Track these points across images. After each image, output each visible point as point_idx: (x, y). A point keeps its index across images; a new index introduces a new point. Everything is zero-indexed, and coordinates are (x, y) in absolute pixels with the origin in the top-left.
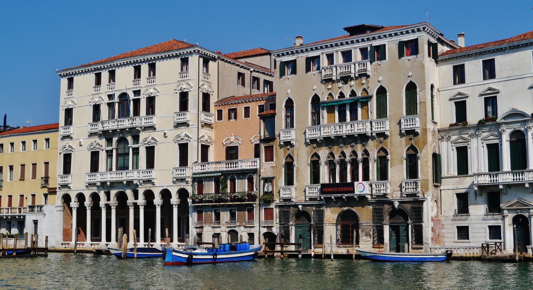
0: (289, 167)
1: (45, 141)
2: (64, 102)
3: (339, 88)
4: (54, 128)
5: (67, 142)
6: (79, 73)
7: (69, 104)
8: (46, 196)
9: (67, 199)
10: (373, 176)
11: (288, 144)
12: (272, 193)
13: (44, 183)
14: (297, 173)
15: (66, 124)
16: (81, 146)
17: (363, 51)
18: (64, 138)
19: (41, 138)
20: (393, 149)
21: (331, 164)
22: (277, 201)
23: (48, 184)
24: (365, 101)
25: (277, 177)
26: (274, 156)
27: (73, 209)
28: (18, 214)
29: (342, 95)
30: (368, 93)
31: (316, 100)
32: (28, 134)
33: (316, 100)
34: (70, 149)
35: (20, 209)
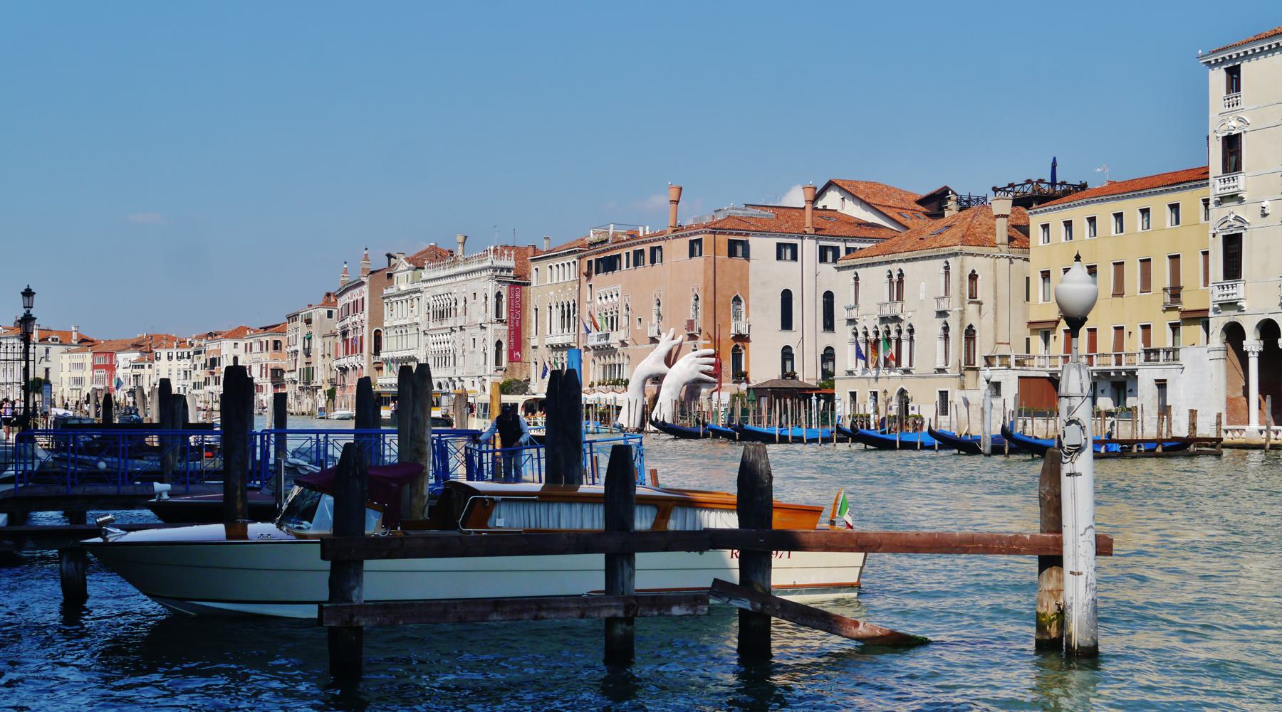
1: (1168, 210)
2: (1220, 122)
4: (1200, 177)
5: (1231, 209)
6: (1255, 54)
7: (1233, 126)
8: (1175, 327)
9: (1234, 334)
13: (1168, 299)
15: (1225, 170)
16: (1265, 215)
18: (1223, 200)
19: (1159, 204)
23: (1179, 302)
27: (1250, 355)
28: (1113, 367)
32: (1128, 197)
34: (1238, 224)
35: (1118, 357)
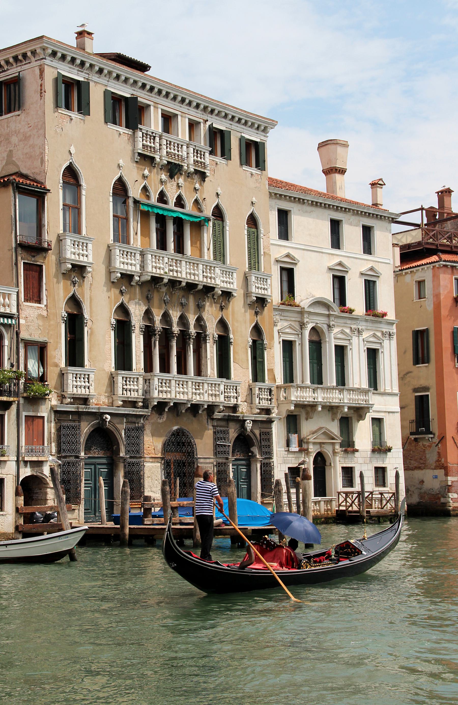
0: (75, 323)
3: (162, 182)
10: (212, 369)
11: (79, 270)
12: (42, 379)
14: (90, 341)
17: (193, 125)
20: (236, 324)
21: (148, 333)
22: (54, 400)
24: (198, 226)
25: (51, 341)
26: (44, 293)
29: (162, 198)
30: (200, 210)
31: (120, 189)
33: (120, 189)
